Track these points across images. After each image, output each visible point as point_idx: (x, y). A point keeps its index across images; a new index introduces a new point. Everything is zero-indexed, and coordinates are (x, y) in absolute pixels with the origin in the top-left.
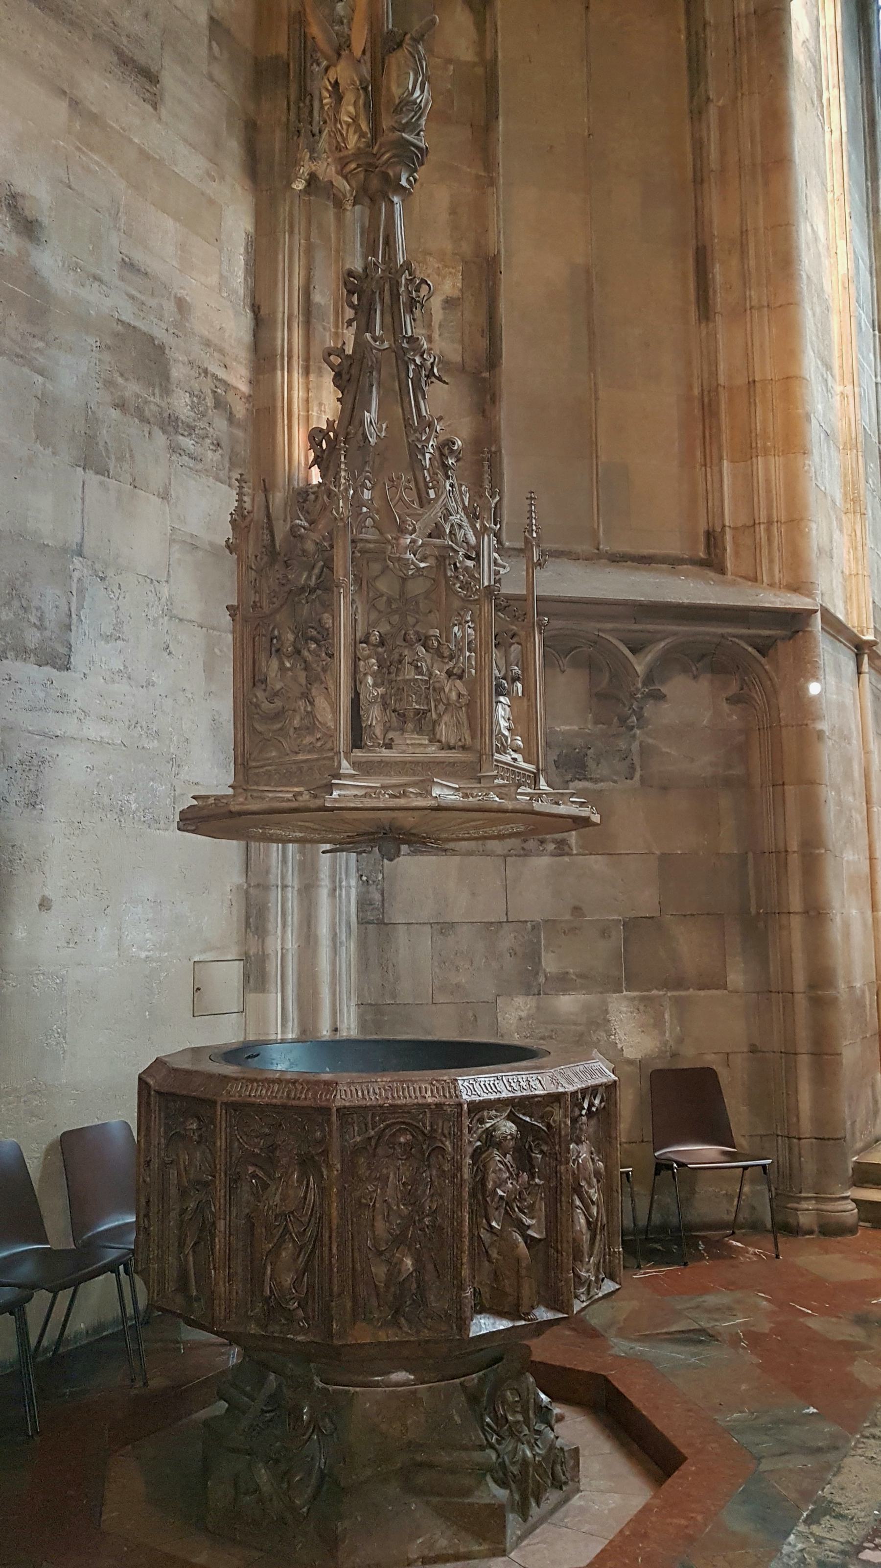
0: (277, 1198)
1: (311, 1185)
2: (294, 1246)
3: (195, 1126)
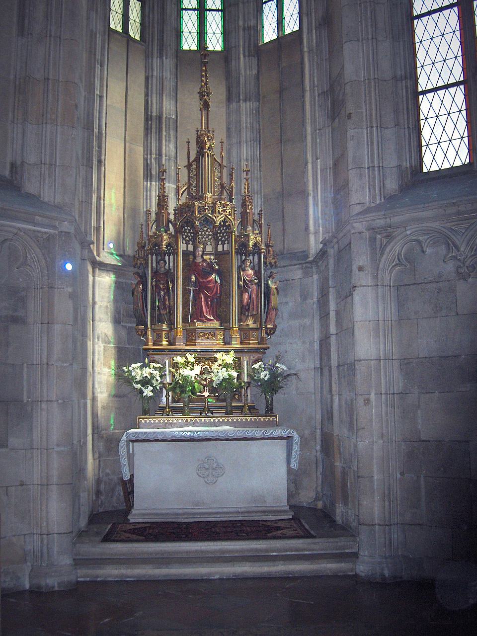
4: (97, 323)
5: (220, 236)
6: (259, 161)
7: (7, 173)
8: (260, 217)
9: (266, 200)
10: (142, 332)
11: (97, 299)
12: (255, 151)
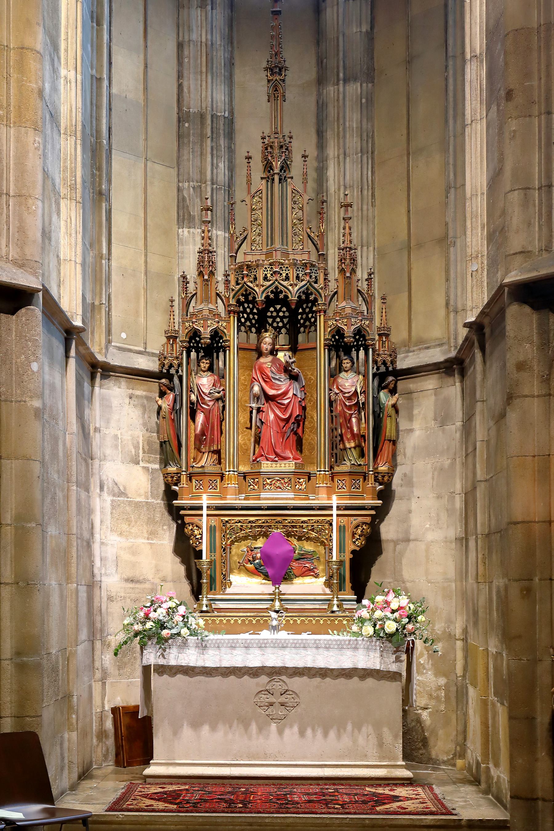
5: (302, 318)
6: (370, 188)
8: (369, 286)
9: (381, 254)
10: (172, 477)
12: (365, 173)
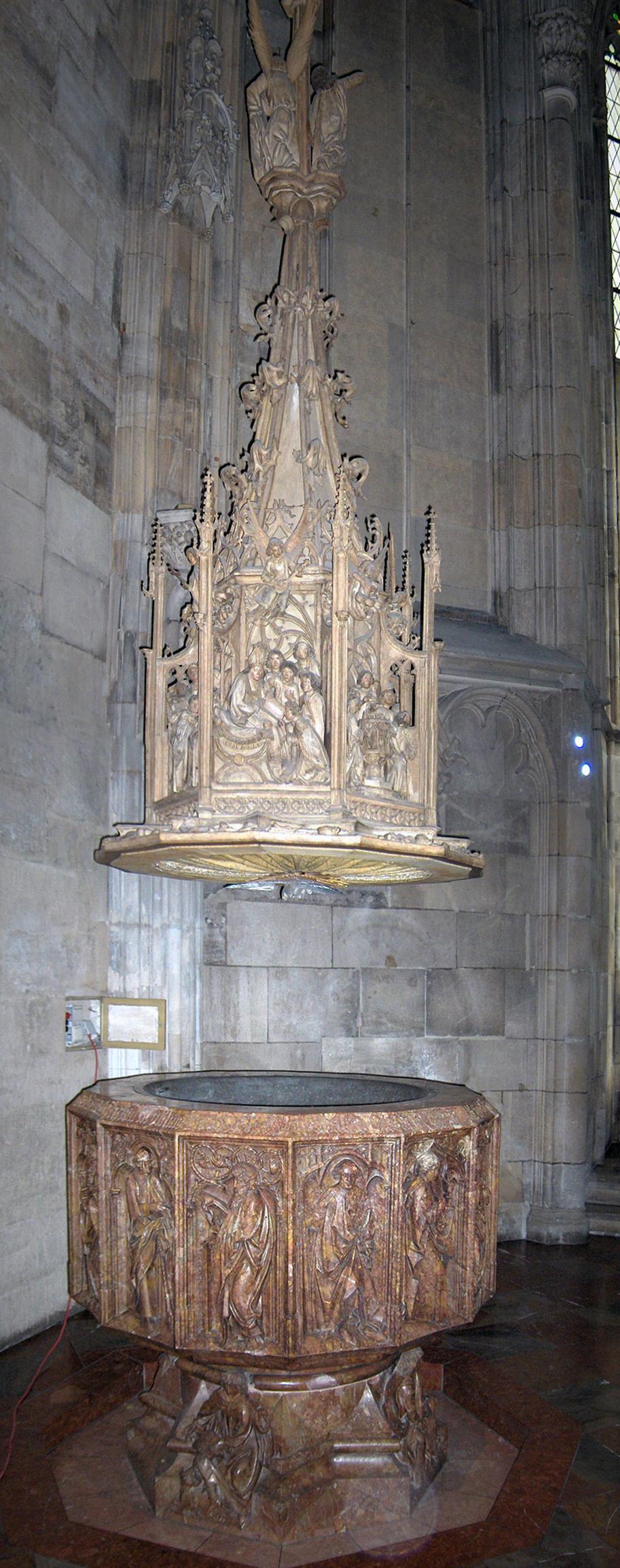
0: (236, 1226)
1: (266, 1215)
2: (252, 1270)
3: (145, 1158)
4: (613, 824)
7: (489, 607)
11: (614, 789)
